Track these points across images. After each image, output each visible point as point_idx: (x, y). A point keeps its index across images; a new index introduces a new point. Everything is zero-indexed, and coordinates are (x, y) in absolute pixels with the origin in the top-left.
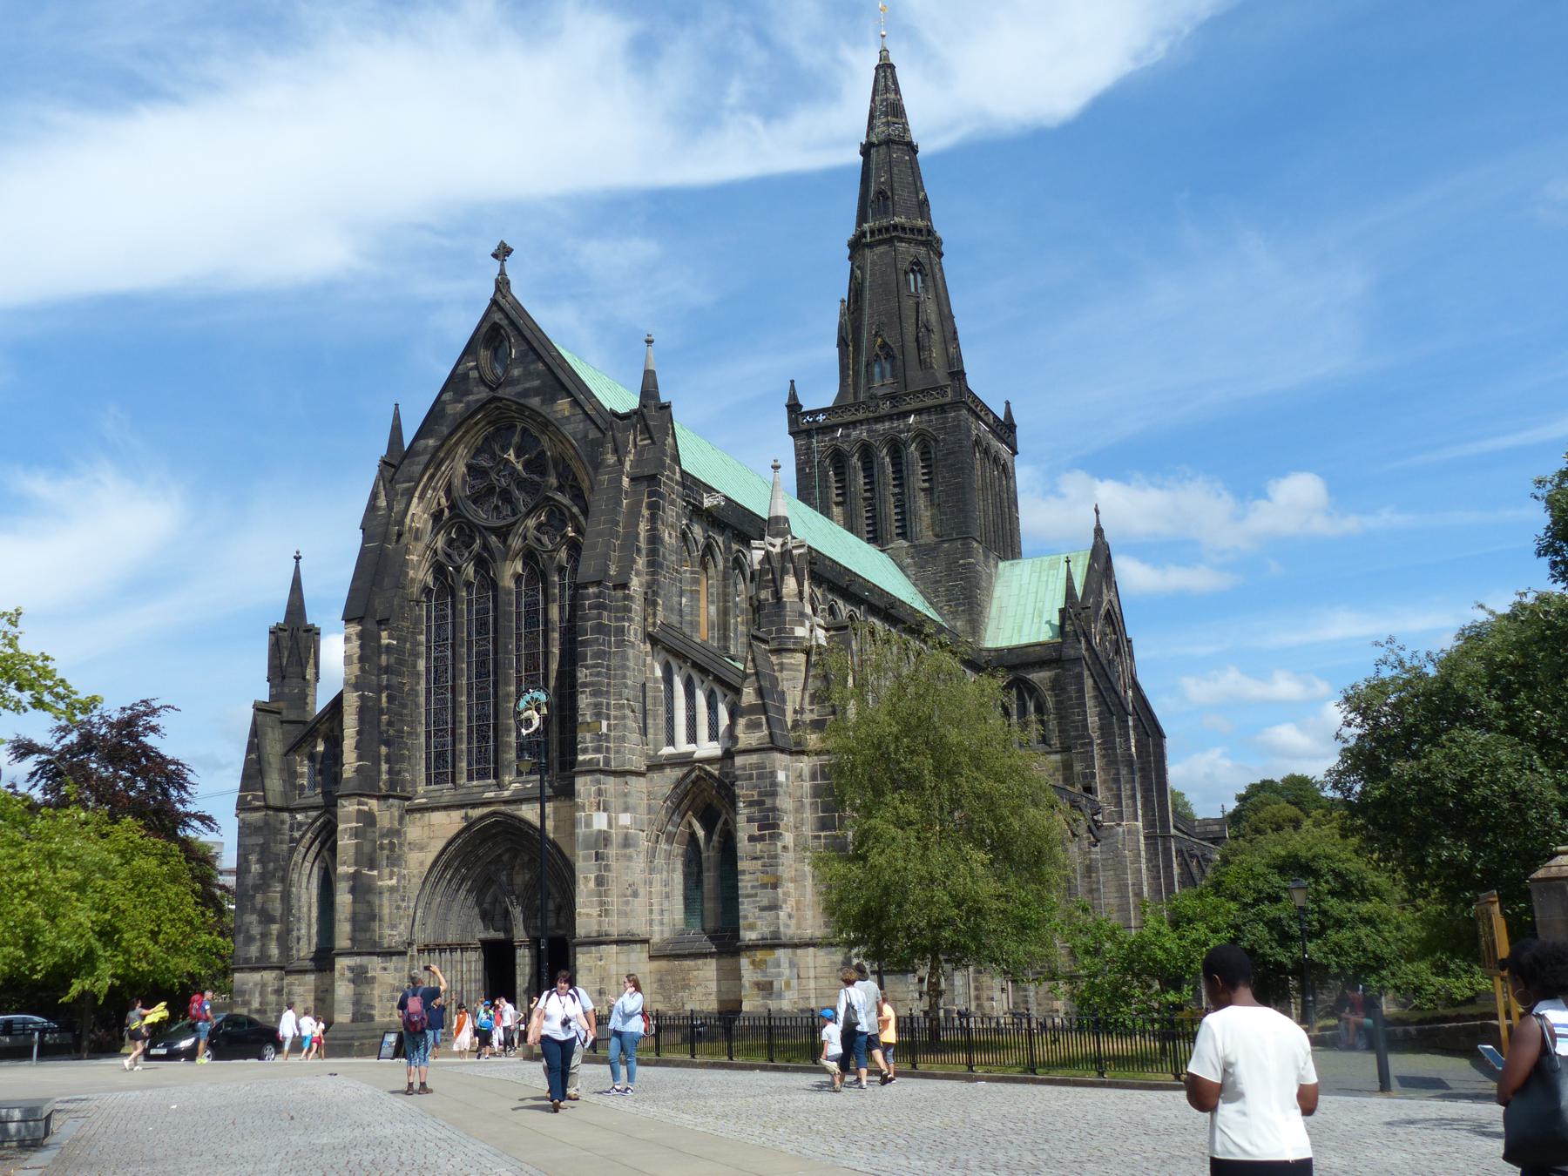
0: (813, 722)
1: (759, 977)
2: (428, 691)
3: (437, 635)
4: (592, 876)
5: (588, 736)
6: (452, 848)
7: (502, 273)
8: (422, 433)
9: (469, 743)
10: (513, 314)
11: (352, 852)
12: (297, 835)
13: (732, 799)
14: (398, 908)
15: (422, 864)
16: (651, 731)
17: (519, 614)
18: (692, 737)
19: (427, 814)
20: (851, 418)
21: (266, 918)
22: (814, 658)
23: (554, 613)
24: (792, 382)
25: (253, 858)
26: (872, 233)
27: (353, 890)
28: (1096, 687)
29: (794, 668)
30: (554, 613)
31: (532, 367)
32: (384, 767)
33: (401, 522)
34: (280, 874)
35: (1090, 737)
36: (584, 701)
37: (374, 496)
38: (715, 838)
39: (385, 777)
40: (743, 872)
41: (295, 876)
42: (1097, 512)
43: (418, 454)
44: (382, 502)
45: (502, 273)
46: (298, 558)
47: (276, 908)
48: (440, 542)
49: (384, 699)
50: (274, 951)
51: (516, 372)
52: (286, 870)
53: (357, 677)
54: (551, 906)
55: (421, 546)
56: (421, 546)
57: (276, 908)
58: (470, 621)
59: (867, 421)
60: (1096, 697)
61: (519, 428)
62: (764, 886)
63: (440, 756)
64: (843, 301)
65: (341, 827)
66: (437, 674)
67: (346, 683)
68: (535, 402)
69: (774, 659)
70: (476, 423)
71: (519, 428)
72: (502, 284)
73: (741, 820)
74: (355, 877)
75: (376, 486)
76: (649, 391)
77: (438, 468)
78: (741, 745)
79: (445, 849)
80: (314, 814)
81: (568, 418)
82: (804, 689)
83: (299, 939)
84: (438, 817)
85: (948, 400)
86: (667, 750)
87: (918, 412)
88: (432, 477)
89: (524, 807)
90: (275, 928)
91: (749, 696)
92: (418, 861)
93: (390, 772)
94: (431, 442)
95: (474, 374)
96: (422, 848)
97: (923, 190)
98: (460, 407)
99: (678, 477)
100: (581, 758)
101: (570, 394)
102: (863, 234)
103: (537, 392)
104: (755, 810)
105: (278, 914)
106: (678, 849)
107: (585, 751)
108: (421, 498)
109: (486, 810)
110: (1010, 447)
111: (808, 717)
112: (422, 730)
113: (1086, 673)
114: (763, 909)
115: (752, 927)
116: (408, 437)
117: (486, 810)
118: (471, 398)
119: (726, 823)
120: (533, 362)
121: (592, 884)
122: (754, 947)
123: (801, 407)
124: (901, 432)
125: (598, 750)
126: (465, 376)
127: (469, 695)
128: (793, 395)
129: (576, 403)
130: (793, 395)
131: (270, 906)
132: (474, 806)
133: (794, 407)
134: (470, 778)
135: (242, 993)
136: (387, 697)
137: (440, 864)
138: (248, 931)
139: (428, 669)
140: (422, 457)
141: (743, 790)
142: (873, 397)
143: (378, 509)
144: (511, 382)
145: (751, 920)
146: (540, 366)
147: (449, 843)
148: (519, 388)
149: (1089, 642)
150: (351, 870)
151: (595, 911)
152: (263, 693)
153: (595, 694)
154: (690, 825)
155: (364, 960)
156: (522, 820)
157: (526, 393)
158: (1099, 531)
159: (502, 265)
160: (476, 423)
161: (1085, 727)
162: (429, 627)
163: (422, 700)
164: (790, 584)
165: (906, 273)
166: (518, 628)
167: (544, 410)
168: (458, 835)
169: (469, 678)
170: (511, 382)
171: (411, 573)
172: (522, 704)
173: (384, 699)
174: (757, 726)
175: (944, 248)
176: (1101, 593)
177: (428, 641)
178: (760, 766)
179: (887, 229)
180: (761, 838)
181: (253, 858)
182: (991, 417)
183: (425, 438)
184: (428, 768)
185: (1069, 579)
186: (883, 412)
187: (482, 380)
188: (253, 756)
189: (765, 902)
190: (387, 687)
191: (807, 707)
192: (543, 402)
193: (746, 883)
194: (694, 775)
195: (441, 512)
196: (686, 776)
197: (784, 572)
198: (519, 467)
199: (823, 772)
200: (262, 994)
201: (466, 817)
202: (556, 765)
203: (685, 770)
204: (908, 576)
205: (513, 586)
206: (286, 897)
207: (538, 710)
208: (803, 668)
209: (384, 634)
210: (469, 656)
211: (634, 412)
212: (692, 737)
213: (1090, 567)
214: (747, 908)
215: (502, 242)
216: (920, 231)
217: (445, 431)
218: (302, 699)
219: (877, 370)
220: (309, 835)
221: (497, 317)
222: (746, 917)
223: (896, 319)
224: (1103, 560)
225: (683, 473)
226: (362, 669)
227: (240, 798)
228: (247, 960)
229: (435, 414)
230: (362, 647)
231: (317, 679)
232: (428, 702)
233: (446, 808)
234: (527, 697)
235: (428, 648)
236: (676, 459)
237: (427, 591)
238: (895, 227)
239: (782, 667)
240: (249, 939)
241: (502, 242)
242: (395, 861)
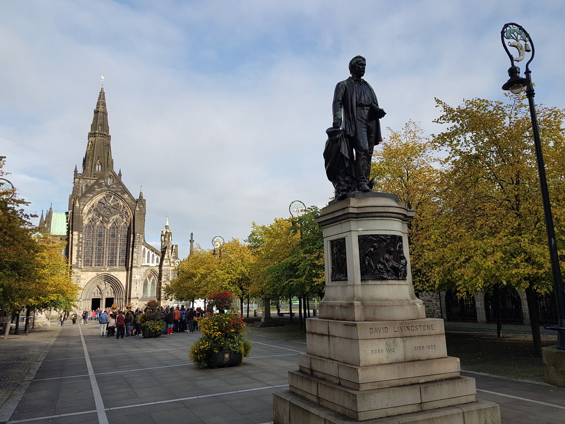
4: (135, 287)
5: (135, 261)
15: (84, 283)
18: (148, 262)
33: (82, 211)
36: (134, 255)
43: (87, 197)
49: (80, 248)
51: (115, 186)
53: (77, 244)
61: (113, 197)
68: (119, 194)
71: (113, 197)
76: (141, 197)
77: (92, 200)
78: (164, 265)
81: (127, 199)
86: (143, 264)
88: (90, 202)
89: (112, 272)
94: (91, 195)
104: (166, 277)
106: (143, 282)
107: (134, 264)
109: (102, 273)
117: (102, 273)
120: (119, 185)
121: (135, 288)
125: (137, 264)
126: (101, 184)
128: (76, 169)
130: (76, 169)
132: (99, 272)
133: (76, 171)
134: (95, 265)
140: (88, 198)
143: (77, 207)
146: (121, 186)
148: (115, 190)
153: (137, 254)
156: (111, 275)
157: (117, 191)
166: (109, 237)
167: (122, 196)
174: (168, 262)
179: (102, 134)
190: (81, 246)
201: (97, 274)
203: (148, 268)
212: (148, 262)
223: (103, 156)
230: (78, 237)
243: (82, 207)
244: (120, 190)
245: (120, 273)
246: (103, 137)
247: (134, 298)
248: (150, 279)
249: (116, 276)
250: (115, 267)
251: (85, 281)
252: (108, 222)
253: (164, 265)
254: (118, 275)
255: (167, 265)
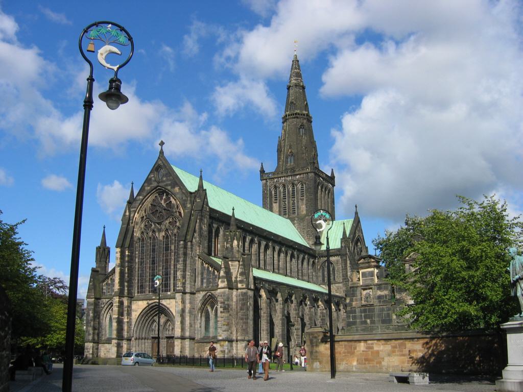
0: (240, 280)
1: (222, 349)
2: (139, 267)
3: (141, 251)
6: (144, 311)
7: (162, 149)
8: (139, 194)
9: (149, 282)
10: (164, 162)
11: (117, 311)
12: (103, 306)
13: (217, 301)
14: (129, 327)
15: (136, 316)
16: (197, 282)
17: (163, 248)
19: (137, 302)
20: (279, 176)
21: (94, 329)
22: (241, 263)
23: (173, 247)
24: (262, 164)
25: (91, 312)
26: (289, 115)
27: (117, 322)
28: (350, 264)
29: (235, 266)
30: (173, 247)
31: (168, 178)
32: (126, 288)
34: (98, 316)
35: (348, 279)
37: (125, 212)
38: (214, 311)
39: (126, 291)
40: (219, 321)
41: (101, 317)
42: (356, 207)
43: (137, 200)
44: (127, 214)
45: (162, 149)
46: (104, 227)
47: (97, 325)
48: (143, 226)
50: (96, 338)
51: (164, 179)
52: (99, 316)
54: (170, 328)
55: (138, 226)
56: (138, 226)
57: (97, 325)
58: (150, 249)
59: (285, 177)
60: (350, 267)
62: (224, 325)
63: (142, 286)
64: (279, 137)
65: (114, 305)
66: (141, 263)
67: (116, 265)
68: (169, 188)
69: (230, 262)
70: (153, 193)
72: (162, 152)
73: (219, 307)
74: (118, 318)
75: (126, 208)
78: (219, 287)
79: (142, 312)
80: (107, 300)
81: (178, 193)
82: (238, 271)
83: (102, 335)
84: (140, 303)
85: (309, 171)
87: (300, 174)
90: (96, 331)
91: (222, 273)
92: (135, 315)
93: (128, 290)
94: (141, 197)
95: (153, 179)
96: (136, 311)
97: (306, 101)
98: (149, 188)
99: (208, 210)
100: (177, 289)
101: (179, 186)
102: (286, 116)
103: (170, 185)
104: (222, 305)
105: (97, 327)
107: (178, 287)
108: (138, 213)
110: (332, 184)
111: (238, 279)
112: (136, 278)
113: (348, 259)
114: (223, 331)
115: (220, 336)
116: (135, 195)
118: (152, 185)
119: (216, 307)
122: (221, 340)
123: (264, 172)
124: (295, 181)
125: (181, 287)
127: (150, 269)
128: (262, 168)
129: (180, 189)
130: (262, 168)
131: (95, 325)
132: (150, 300)
134: (149, 292)
135: (87, 349)
136: (128, 269)
137: (141, 316)
138: (89, 332)
139: (139, 262)
141: (220, 299)
142: (286, 169)
144: (163, 182)
145: (220, 334)
147: (143, 310)
148: (165, 184)
149: (349, 249)
150: (117, 316)
151: (180, 330)
152: (94, 265)
154: (207, 307)
155: (120, 341)
157: (167, 185)
158: (356, 213)
159: (162, 148)
160: (153, 193)
161: (347, 276)
162: (139, 250)
163: (137, 270)
164: (235, 242)
165: (300, 129)
166: (163, 251)
167: (172, 190)
168: (146, 308)
169: (150, 264)
170: (163, 182)
171: (135, 234)
172: (155, 279)
173: (126, 270)
174: (224, 282)
175: (312, 120)
176: (355, 233)
177: (139, 253)
178: (224, 293)
180: (224, 312)
181: (91, 312)
182: (324, 175)
183: (140, 196)
184: (138, 289)
185: (344, 229)
186: (289, 174)
187: (155, 181)
188: (91, 284)
189: (224, 329)
191: (238, 276)
192: (171, 188)
193: (219, 324)
194: (208, 294)
195: (144, 217)
196: (206, 294)
197: (234, 239)
198: (164, 205)
199: (242, 295)
200: (93, 349)
201: (148, 303)
202: (172, 290)
204: (295, 227)
205: (162, 239)
206: (99, 323)
207: (159, 280)
208: (238, 266)
209: (127, 252)
210: (150, 258)
211: (196, 191)
213: (353, 225)
214: (219, 330)
215: (162, 141)
216: (304, 115)
217: (145, 195)
218: (106, 267)
219: (289, 160)
220: (106, 306)
221: (160, 162)
222: (219, 333)
224: (357, 222)
225: (210, 209)
226: (121, 262)
227: (87, 295)
228: (89, 340)
229: (142, 189)
230: (121, 255)
231: (109, 262)
232: (138, 271)
233: (142, 300)
234: (156, 277)
235: (139, 256)
236: (207, 205)
237: (139, 239)
238: (296, 114)
239: (232, 265)
240: (89, 334)
241: (162, 141)
242: (129, 314)
243: (132, 215)
244: (169, 182)
245: (171, 300)
246: (295, 118)
247: (178, 338)
248: (212, 310)
249: (168, 306)
250: (169, 293)
251: (136, 313)
252: (160, 231)
253: (219, 287)
254: (169, 304)
255: (223, 286)
